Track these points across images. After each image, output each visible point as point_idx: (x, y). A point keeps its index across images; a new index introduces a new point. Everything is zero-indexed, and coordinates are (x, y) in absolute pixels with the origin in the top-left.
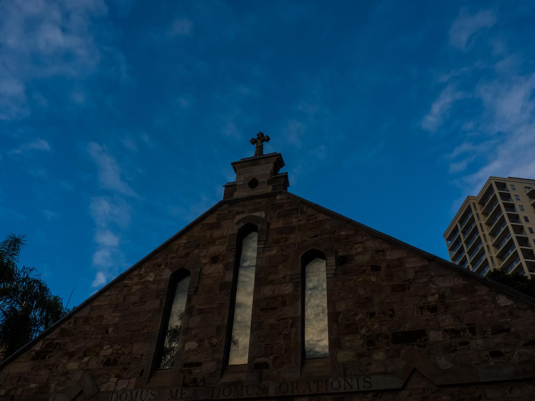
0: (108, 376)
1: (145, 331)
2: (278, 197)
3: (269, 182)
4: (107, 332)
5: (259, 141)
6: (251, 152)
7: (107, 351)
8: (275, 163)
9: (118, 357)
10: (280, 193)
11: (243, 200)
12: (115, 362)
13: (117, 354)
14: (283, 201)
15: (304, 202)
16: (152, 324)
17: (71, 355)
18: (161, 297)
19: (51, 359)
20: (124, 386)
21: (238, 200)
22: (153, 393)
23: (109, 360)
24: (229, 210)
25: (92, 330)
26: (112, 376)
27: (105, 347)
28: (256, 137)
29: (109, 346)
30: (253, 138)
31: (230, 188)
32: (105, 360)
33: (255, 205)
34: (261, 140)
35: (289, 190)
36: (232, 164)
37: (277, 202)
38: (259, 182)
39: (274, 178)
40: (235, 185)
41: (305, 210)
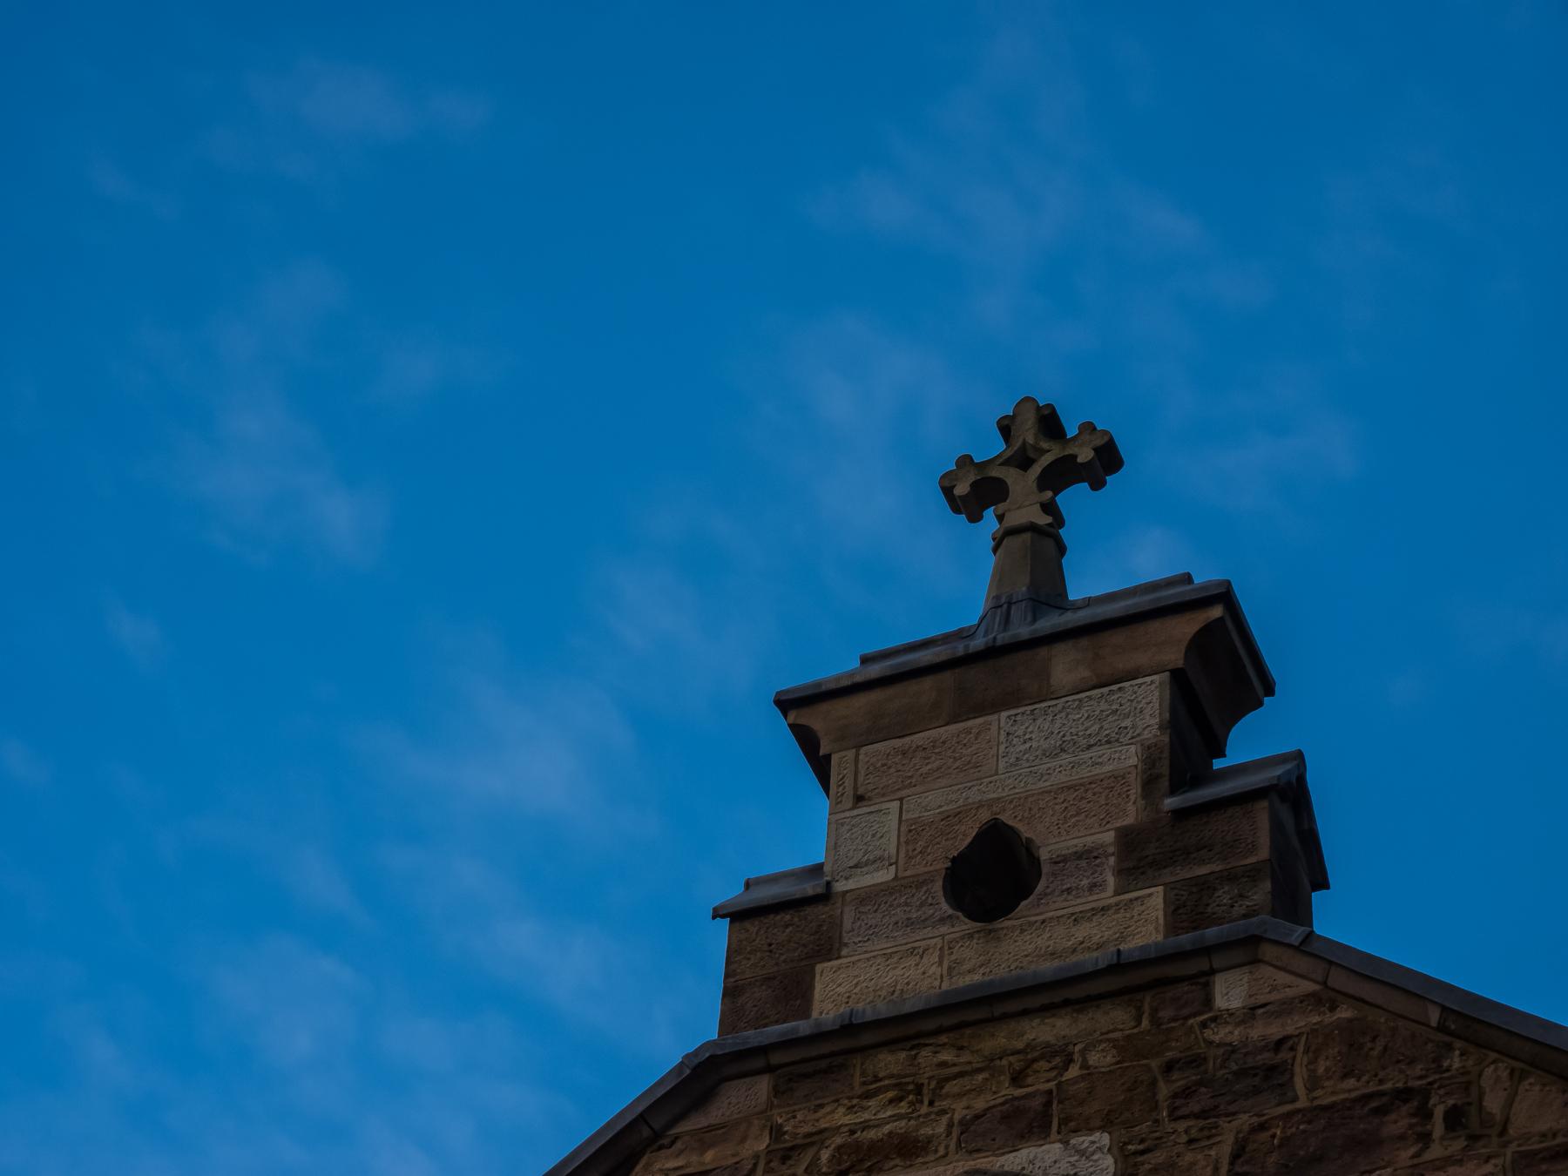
2: (1230, 992)
3: (1138, 856)
5: (1022, 484)
6: (949, 581)
8: (1178, 678)
10: (1247, 949)
11: (906, 1028)
14: (1275, 1031)
15: (1473, 1025)
21: (856, 1036)
24: (777, 1132)
28: (992, 446)
30: (965, 461)
31: (780, 927)
33: (1017, 1079)
34: (1039, 465)
35: (1336, 917)
36: (785, 703)
37: (1219, 1034)
38: (1044, 855)
39: (1180, 814)
40: (825, 897)
41: (1494, 1104)
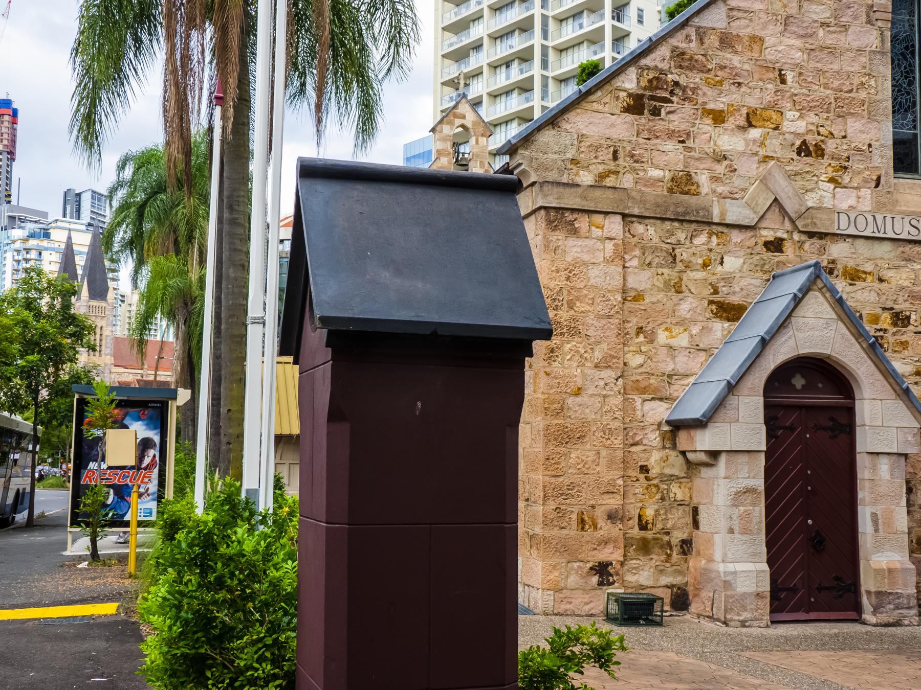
0: (815, 178)
1: (863, 95)
4: (783, 82)
7: (796, 124)
9: (822, 141)
12: (820, 152)
13: (819, 134)
16: (873, 83)
17: (718, 118)
18: (879, 24)
19: (671, 117)
20: (852, 201)
22: (914, 222)
23: (804, 142)
25: (746, 67)
26: (822, 178)
27: (790, 115)
29: (798, 114)
32: (798, 143)
